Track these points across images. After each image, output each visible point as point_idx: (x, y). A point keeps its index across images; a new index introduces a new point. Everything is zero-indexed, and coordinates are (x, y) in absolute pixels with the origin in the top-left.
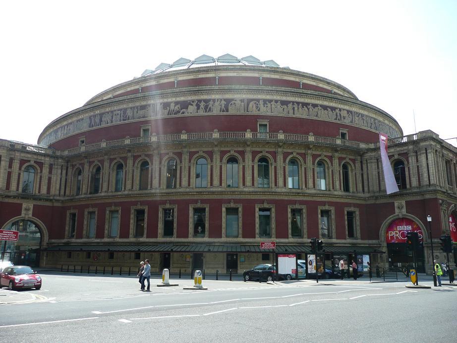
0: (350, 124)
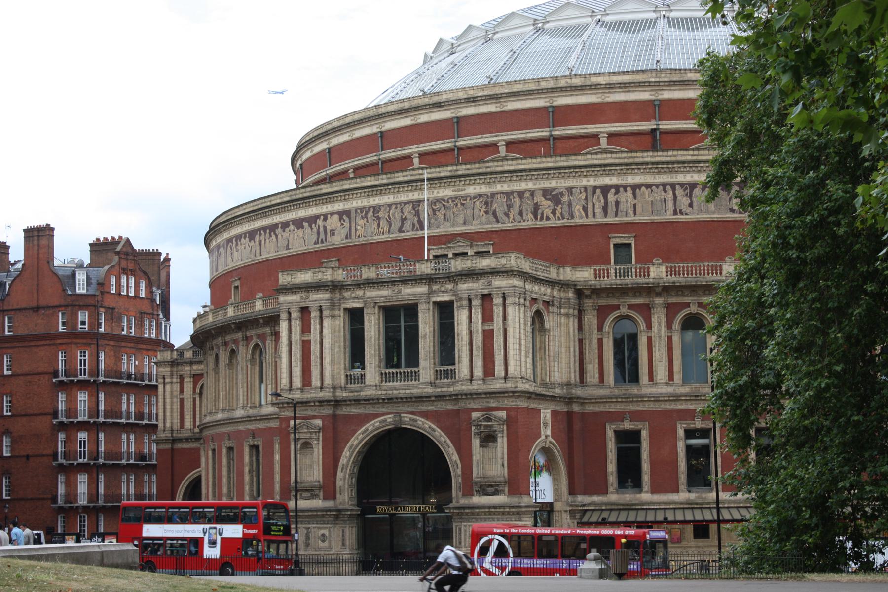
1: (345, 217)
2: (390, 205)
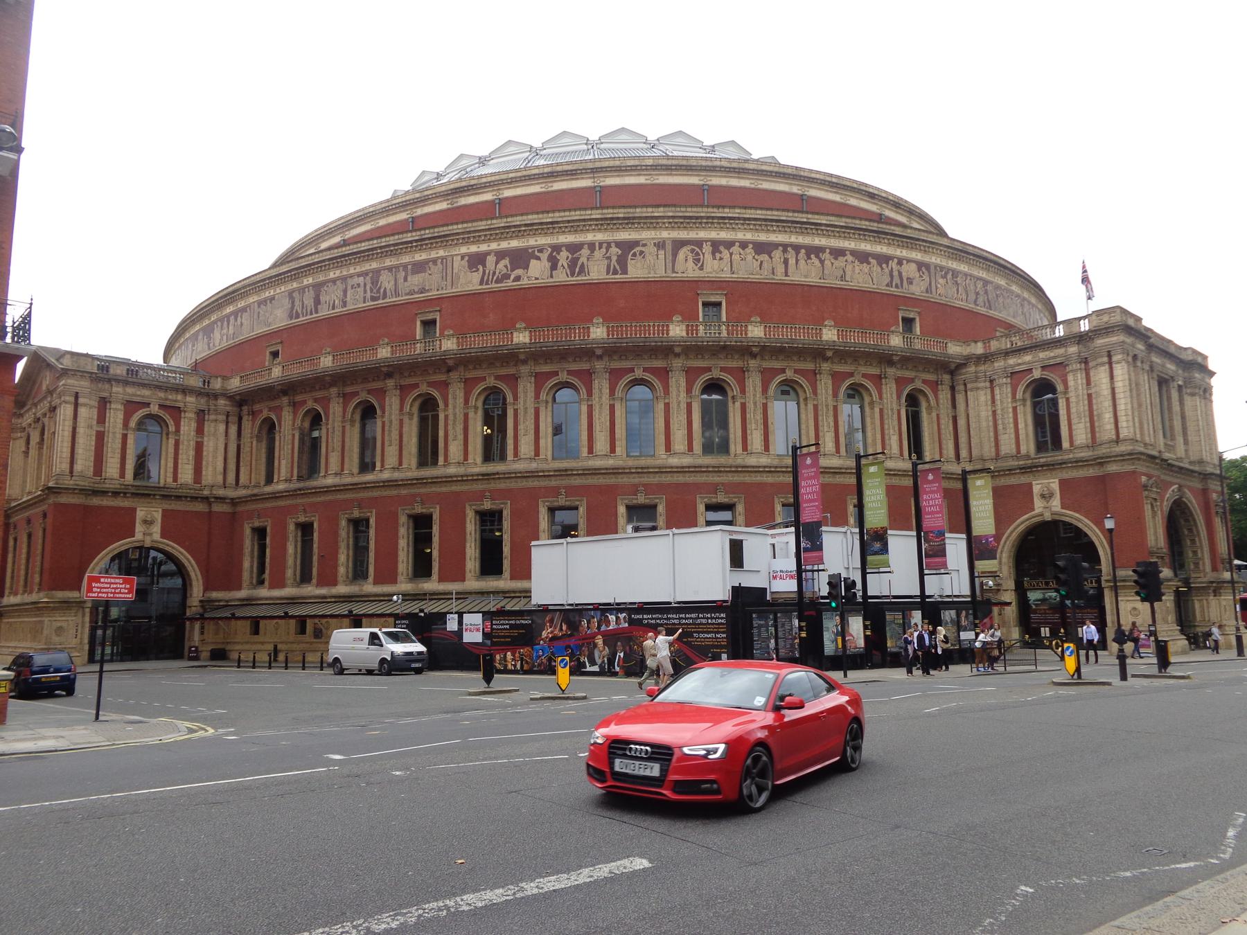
0: (925, 296)
2: (966, 275)
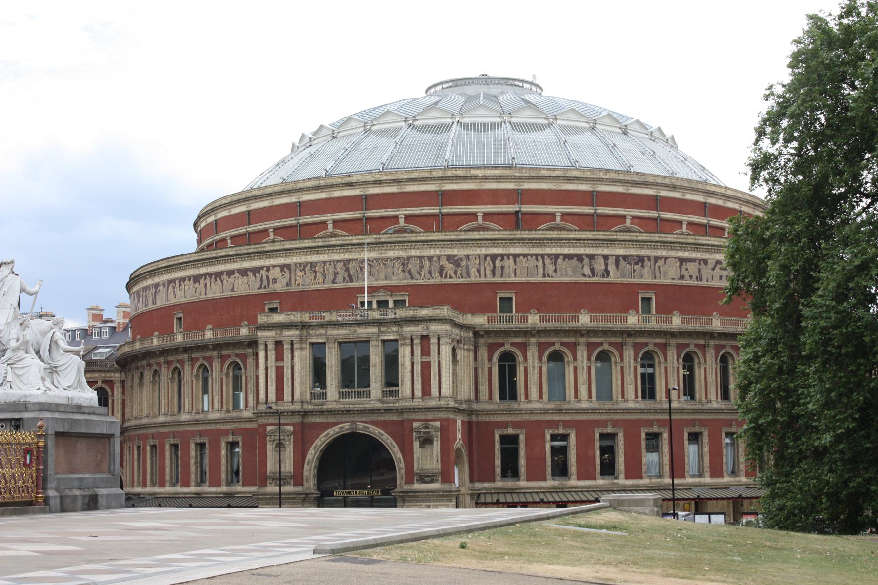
0: (286, 289)
1: (285, 269)
2: (325, 263)
